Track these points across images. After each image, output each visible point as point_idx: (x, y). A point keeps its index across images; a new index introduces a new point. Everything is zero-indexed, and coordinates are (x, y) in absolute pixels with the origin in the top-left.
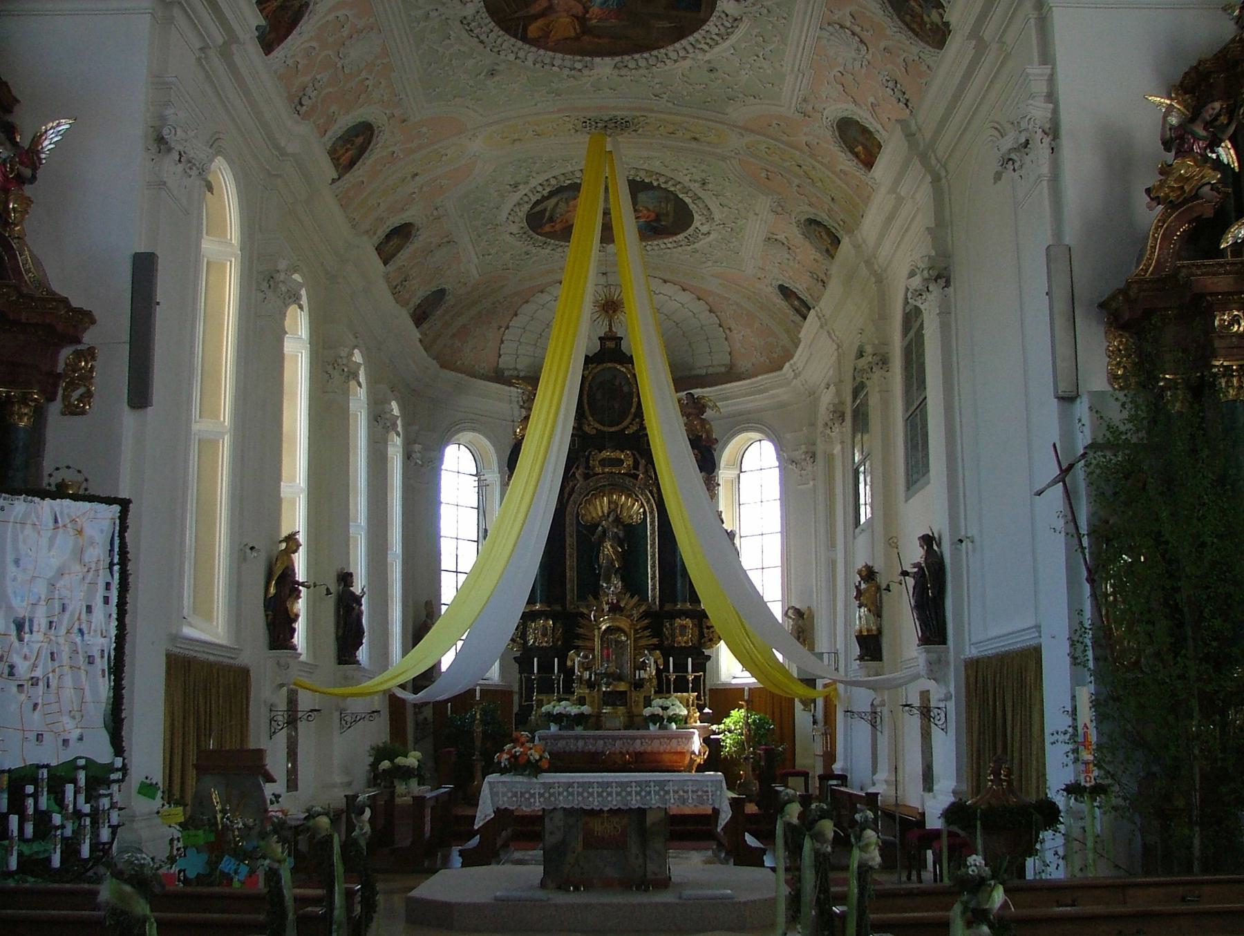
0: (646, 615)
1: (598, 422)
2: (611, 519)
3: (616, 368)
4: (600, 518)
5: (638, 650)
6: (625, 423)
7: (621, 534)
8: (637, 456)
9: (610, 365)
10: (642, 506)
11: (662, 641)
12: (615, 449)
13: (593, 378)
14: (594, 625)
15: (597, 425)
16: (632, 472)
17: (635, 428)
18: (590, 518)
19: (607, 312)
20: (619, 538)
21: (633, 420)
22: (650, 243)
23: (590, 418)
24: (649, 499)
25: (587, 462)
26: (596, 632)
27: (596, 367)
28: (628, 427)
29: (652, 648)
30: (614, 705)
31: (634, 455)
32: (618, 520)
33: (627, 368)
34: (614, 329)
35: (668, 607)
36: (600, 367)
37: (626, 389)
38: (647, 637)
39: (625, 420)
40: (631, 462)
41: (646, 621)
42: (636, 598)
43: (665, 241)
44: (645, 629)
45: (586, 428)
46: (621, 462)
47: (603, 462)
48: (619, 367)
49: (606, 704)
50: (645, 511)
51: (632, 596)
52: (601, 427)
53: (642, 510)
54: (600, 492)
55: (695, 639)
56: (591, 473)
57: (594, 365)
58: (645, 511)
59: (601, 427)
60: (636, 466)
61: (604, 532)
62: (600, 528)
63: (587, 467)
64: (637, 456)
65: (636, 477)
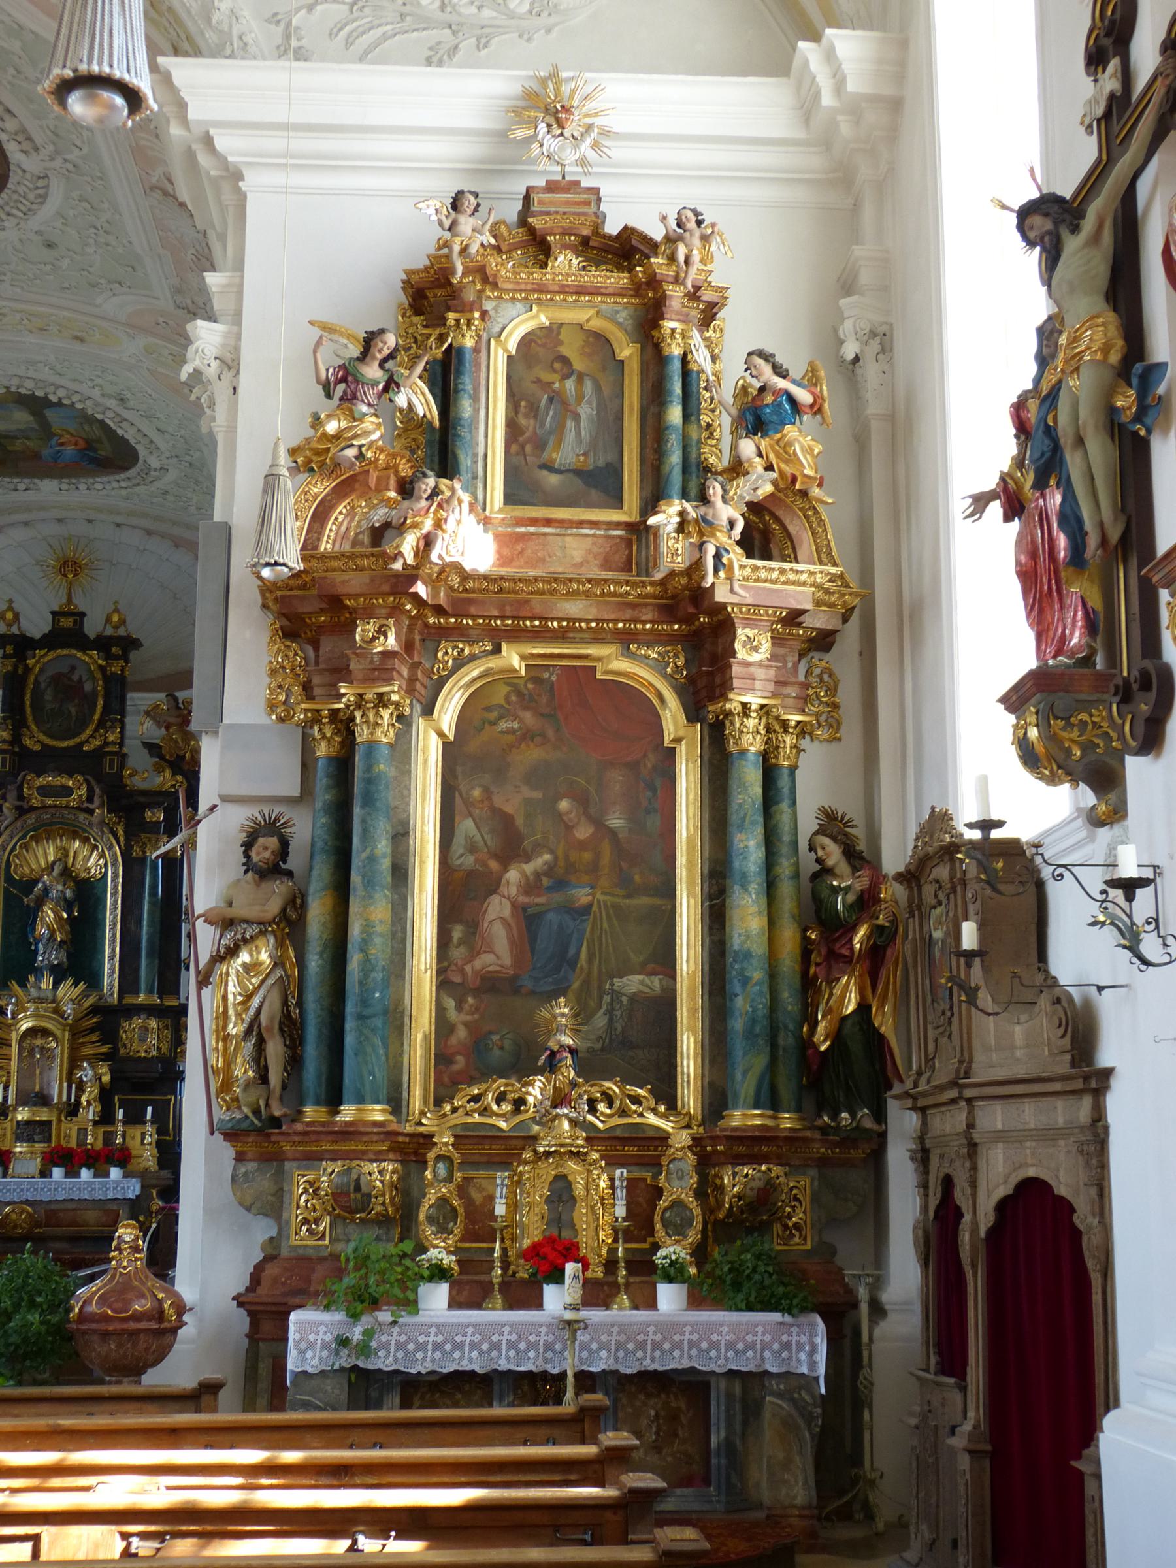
0: (95, 1010)
1: (46, 734)
2: (55, 873)
3: (75, 656)
4: (43, 870)
5: (74, 1064)
6: (83, 737)
7: (68, 893)
8: (93, 782)
9: (66, 652)
10: (102, 855)
11: (115, 1049)
12: (60, 771)
13: (42, 670)
14: (10, 1026)
15: (42, 737)
16: (85, 805)
17: (97, 743)
18: (27, 871)
19: (65, 575)
20: (65, 900)
21: (96, 730)
22: (98, 479)
23: (33, 727)
24: (112, 844)
25: (20, 788)
26: (14, 1034)
27: (45, 655)
28: (87, 741)
29: (95, 1060)
30: (30, 1140)
31: (86, 780)
32: (66, 873)
33: (91, 657)
34: (75, 601)
35: (129, 1000)
36: (51, 655)
37: (88, 687)
38: (94, 1042)
39: (84, 730)
40: (83, 791)
41: (94, 1020)
42: (82, 985)
43: (117, 477)
44: (92, 1030)
45: (28, 742)
46: (68, 791)
47: (45, 791)
48: (79, 654)
49: (18, 1138)
50: (106, 865)
51: (76, 984)
52: (47, 741)
53: (101, 862)
54: (43, 831)
55: (165, 1048)
56: (25, 806)
57: (43, 652)
58: (106, 865)
59: (47, 741)
60: (90, 799)
61: (46, 891)
62: (40, 885)
63: (21, 797)
64: (93, 782)
65: (91, 812)
